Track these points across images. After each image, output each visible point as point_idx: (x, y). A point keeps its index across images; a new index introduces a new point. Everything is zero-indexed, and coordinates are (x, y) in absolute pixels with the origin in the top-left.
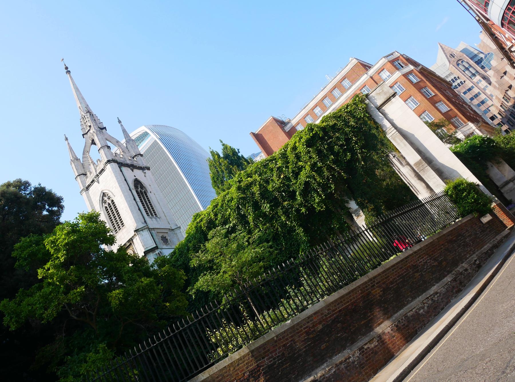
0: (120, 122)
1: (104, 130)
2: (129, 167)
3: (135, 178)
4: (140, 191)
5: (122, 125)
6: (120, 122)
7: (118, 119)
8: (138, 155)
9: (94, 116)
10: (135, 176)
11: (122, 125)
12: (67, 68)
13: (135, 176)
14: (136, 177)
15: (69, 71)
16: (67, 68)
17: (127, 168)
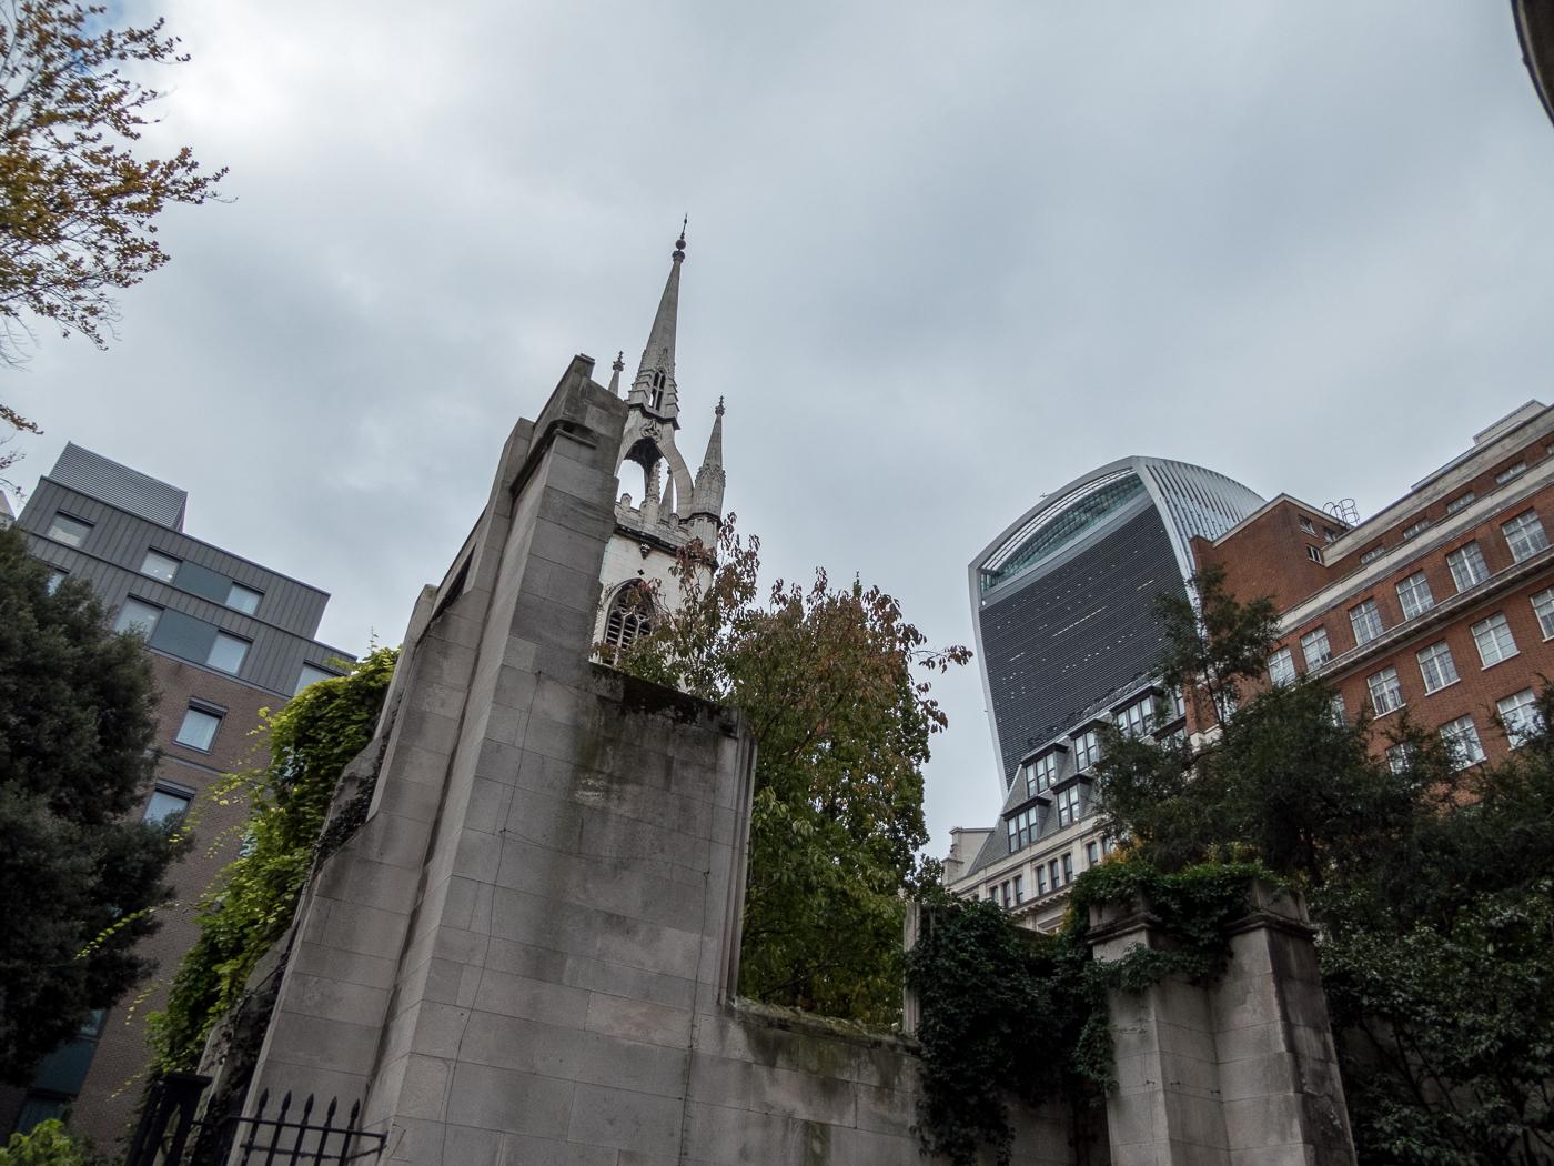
0: (720, 411)
1: (670, 426)
2: (640, 542)
3: (638, 576)
4: (631, 620)
5: (718, 421)
6: (720, 411)
7: (721, 402)
8: (703, 514)
9: (668, 382)
10: (641, 572)
11: (718, 421)
12: (681, 244)
13: (641, 572)
14: (642, 577)
15: (683, 256)
16: (681, 244)
17: (629, 542)
